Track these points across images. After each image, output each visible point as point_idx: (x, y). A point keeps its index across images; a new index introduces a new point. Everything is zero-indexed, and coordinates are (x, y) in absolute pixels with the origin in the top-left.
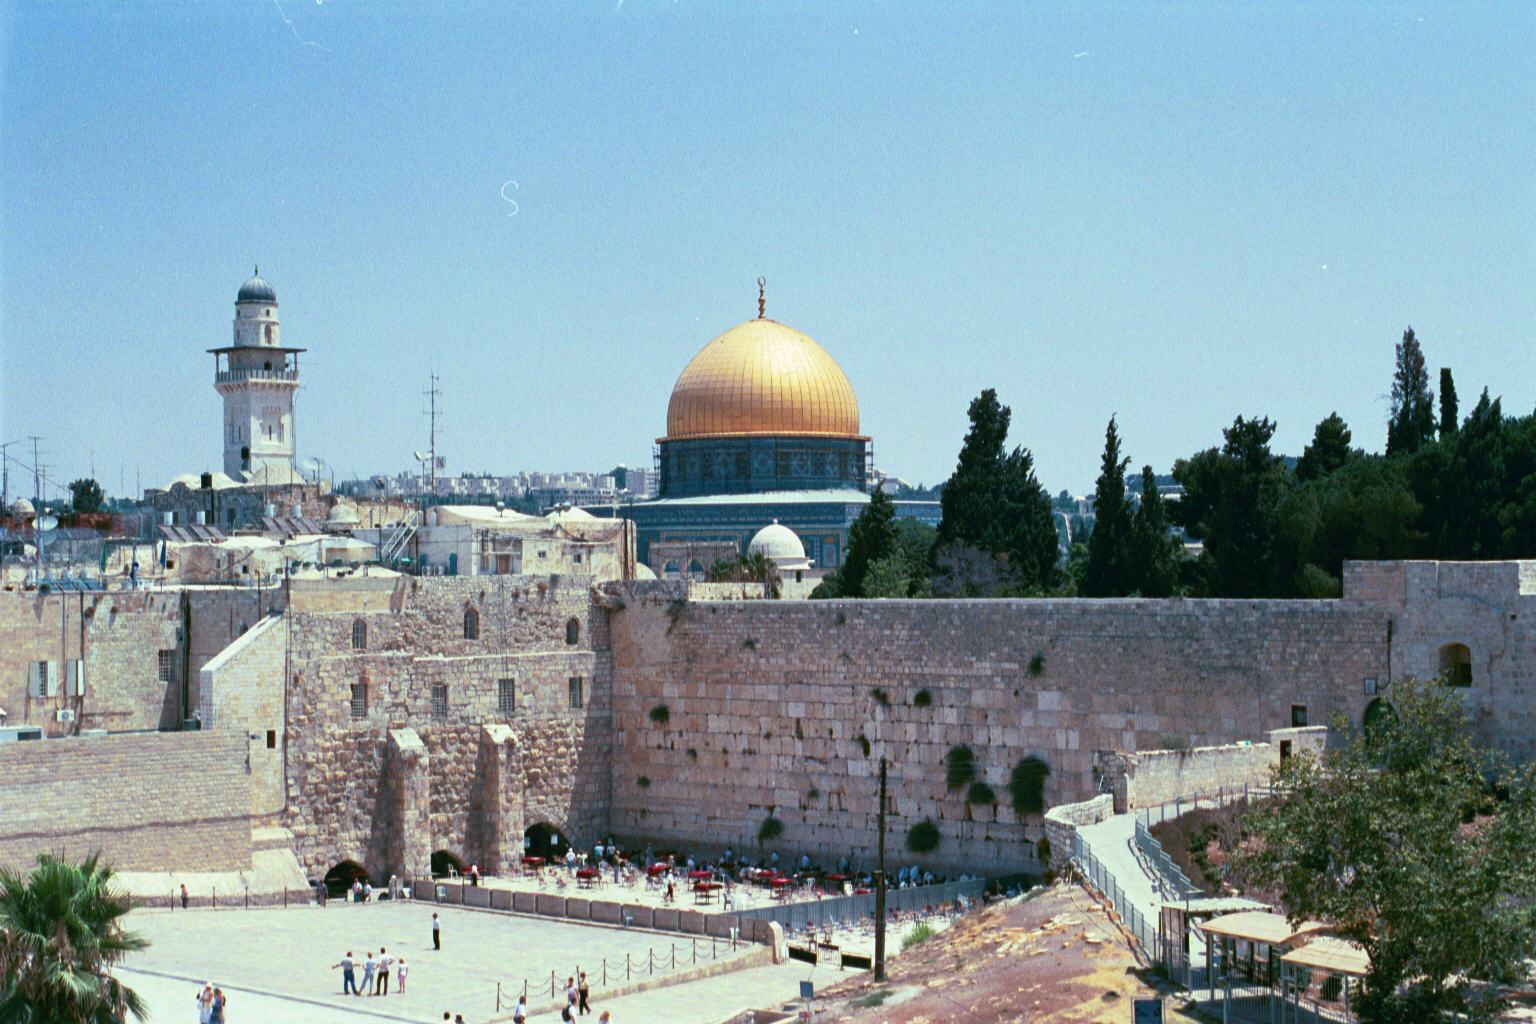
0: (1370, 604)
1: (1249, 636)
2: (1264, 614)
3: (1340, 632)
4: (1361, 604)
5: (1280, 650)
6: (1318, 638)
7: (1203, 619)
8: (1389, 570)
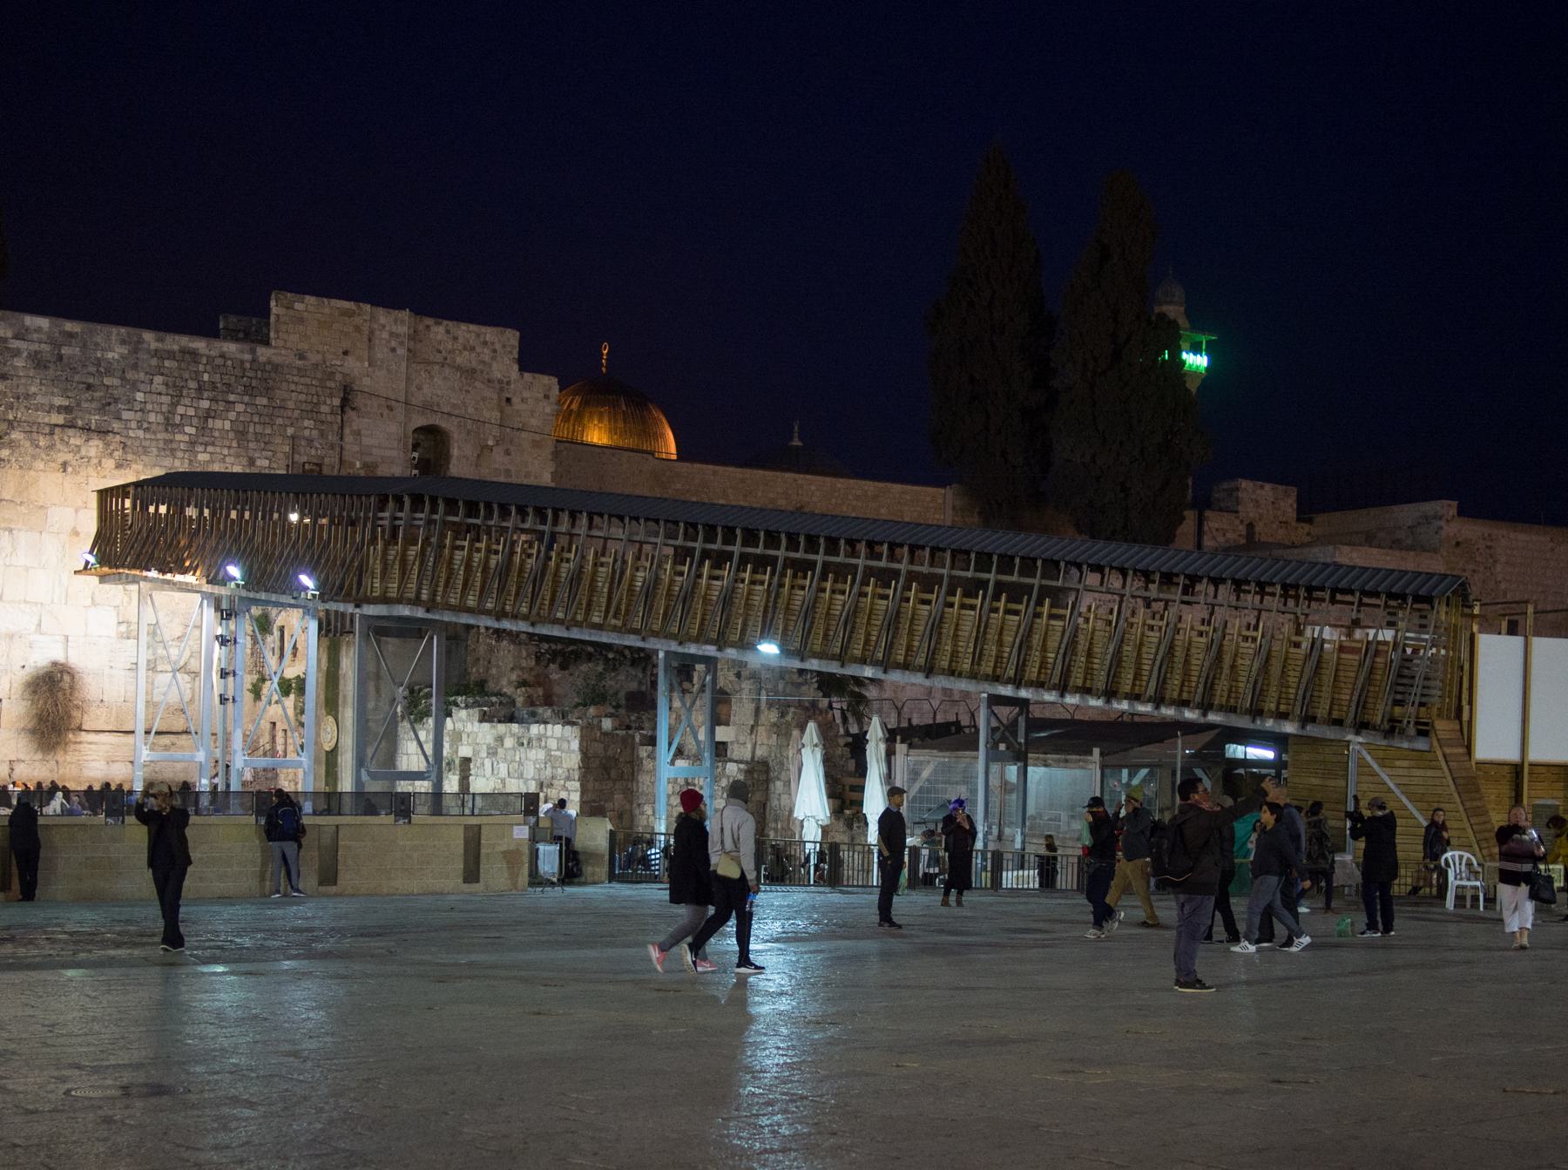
0: (314, 358)
1: (107, 381)
2: (136, 351)
3: (268, 391)
4: (302, 357)
5: (165, 408)
6: (232, 398)
7: (15, 344)
8: (349, 314)
